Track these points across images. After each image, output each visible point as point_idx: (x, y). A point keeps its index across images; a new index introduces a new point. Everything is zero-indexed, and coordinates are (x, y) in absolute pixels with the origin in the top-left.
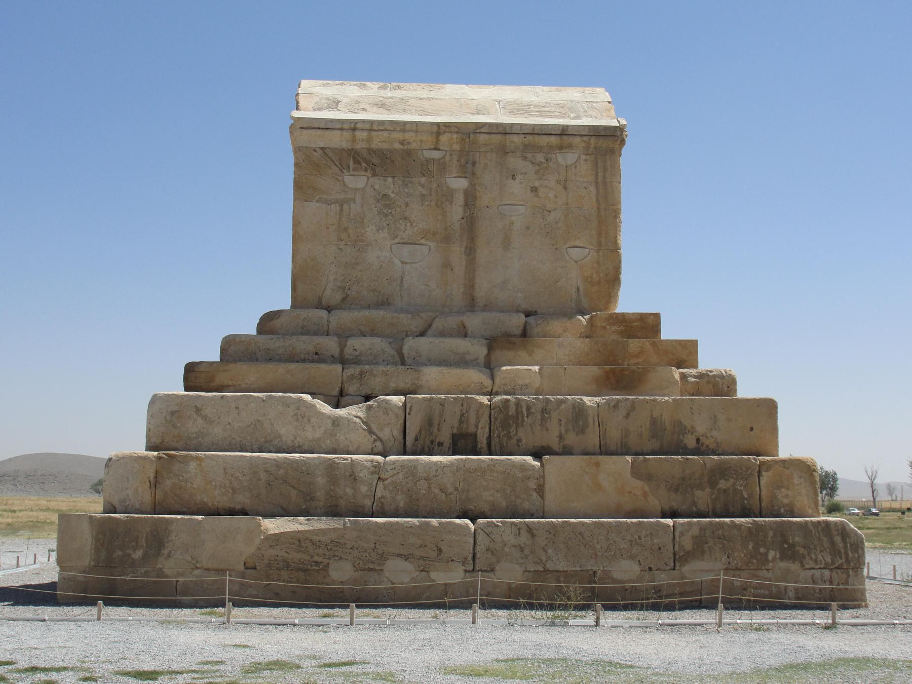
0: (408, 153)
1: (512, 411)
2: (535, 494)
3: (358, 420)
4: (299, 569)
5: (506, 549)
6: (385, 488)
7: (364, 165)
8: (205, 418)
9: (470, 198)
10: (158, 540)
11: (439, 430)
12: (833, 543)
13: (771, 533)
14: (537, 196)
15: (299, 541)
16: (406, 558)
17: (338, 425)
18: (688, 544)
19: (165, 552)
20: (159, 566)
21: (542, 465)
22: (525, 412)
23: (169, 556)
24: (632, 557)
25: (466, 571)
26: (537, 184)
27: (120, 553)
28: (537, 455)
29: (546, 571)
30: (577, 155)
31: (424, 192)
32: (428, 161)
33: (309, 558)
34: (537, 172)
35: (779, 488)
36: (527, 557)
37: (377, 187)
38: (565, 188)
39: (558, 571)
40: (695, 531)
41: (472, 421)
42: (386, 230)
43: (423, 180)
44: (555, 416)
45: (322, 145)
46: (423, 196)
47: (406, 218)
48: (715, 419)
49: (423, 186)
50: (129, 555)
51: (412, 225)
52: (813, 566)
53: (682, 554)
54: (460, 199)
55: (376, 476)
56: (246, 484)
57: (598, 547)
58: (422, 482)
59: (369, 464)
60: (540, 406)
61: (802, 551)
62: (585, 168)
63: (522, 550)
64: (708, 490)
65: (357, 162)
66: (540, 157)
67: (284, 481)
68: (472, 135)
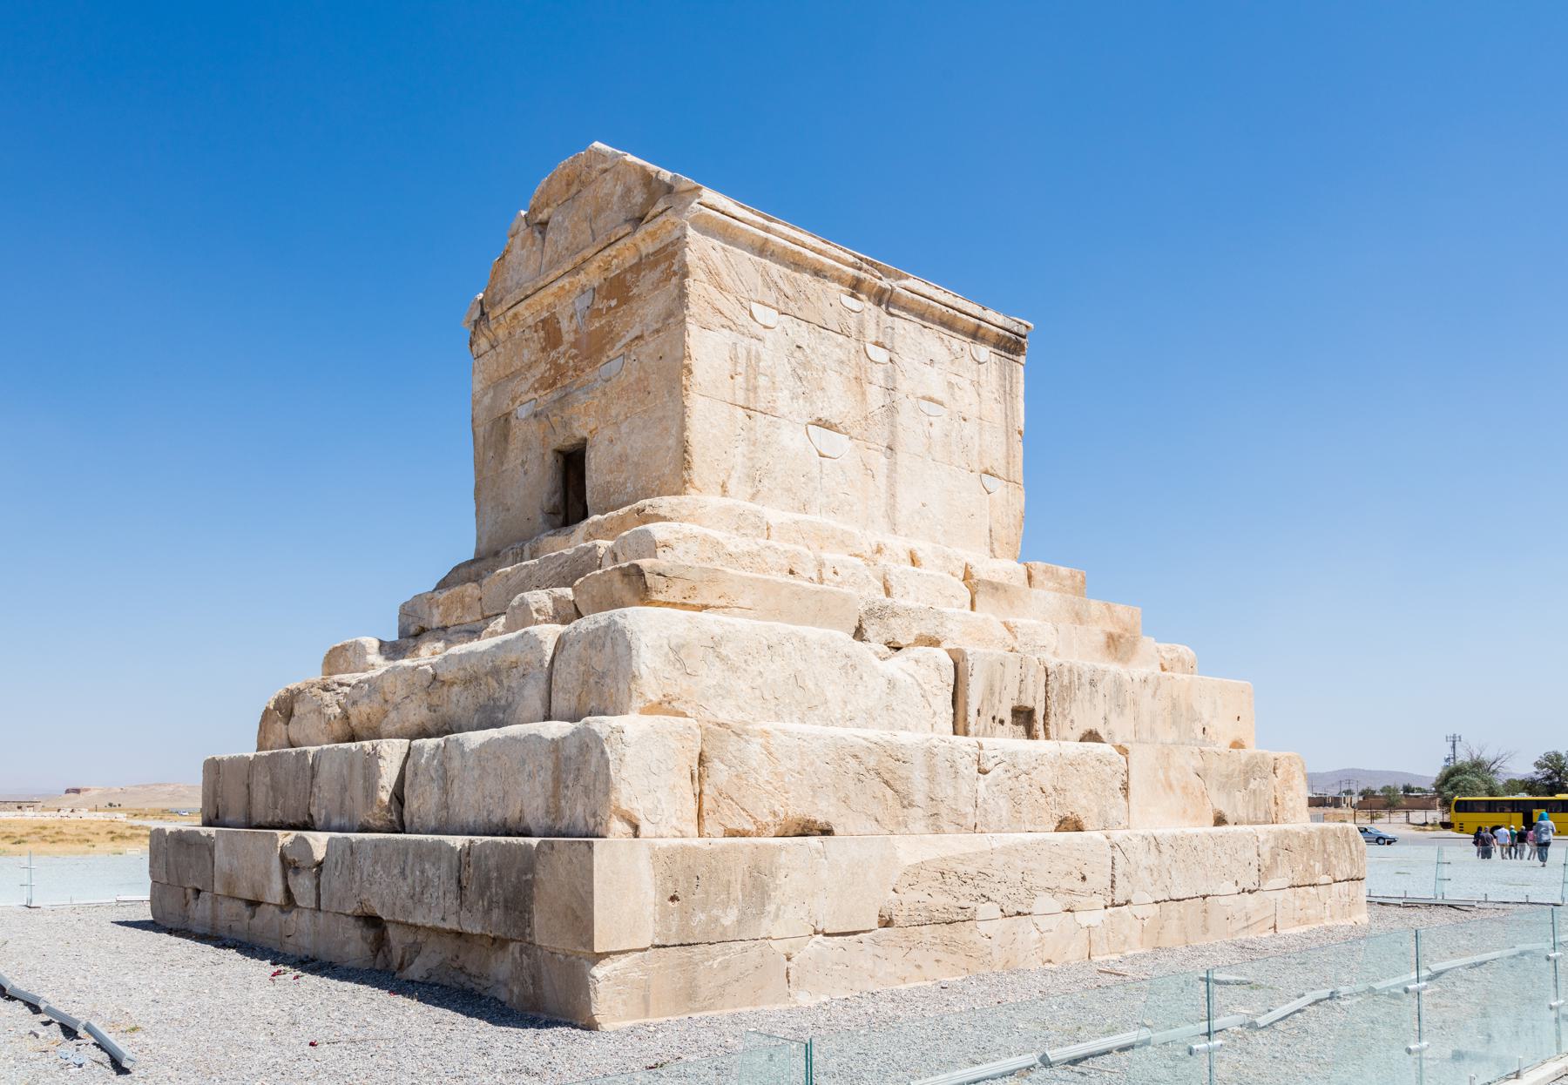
3: (909, 680)
19: (771, 908)
23: (777, 916)
26: (954, 379)
27: (703, 917)
43: (841, 338)
49: (840, 346)
50: (717, 920)
54: (878, 376)
58: (1023, 777)
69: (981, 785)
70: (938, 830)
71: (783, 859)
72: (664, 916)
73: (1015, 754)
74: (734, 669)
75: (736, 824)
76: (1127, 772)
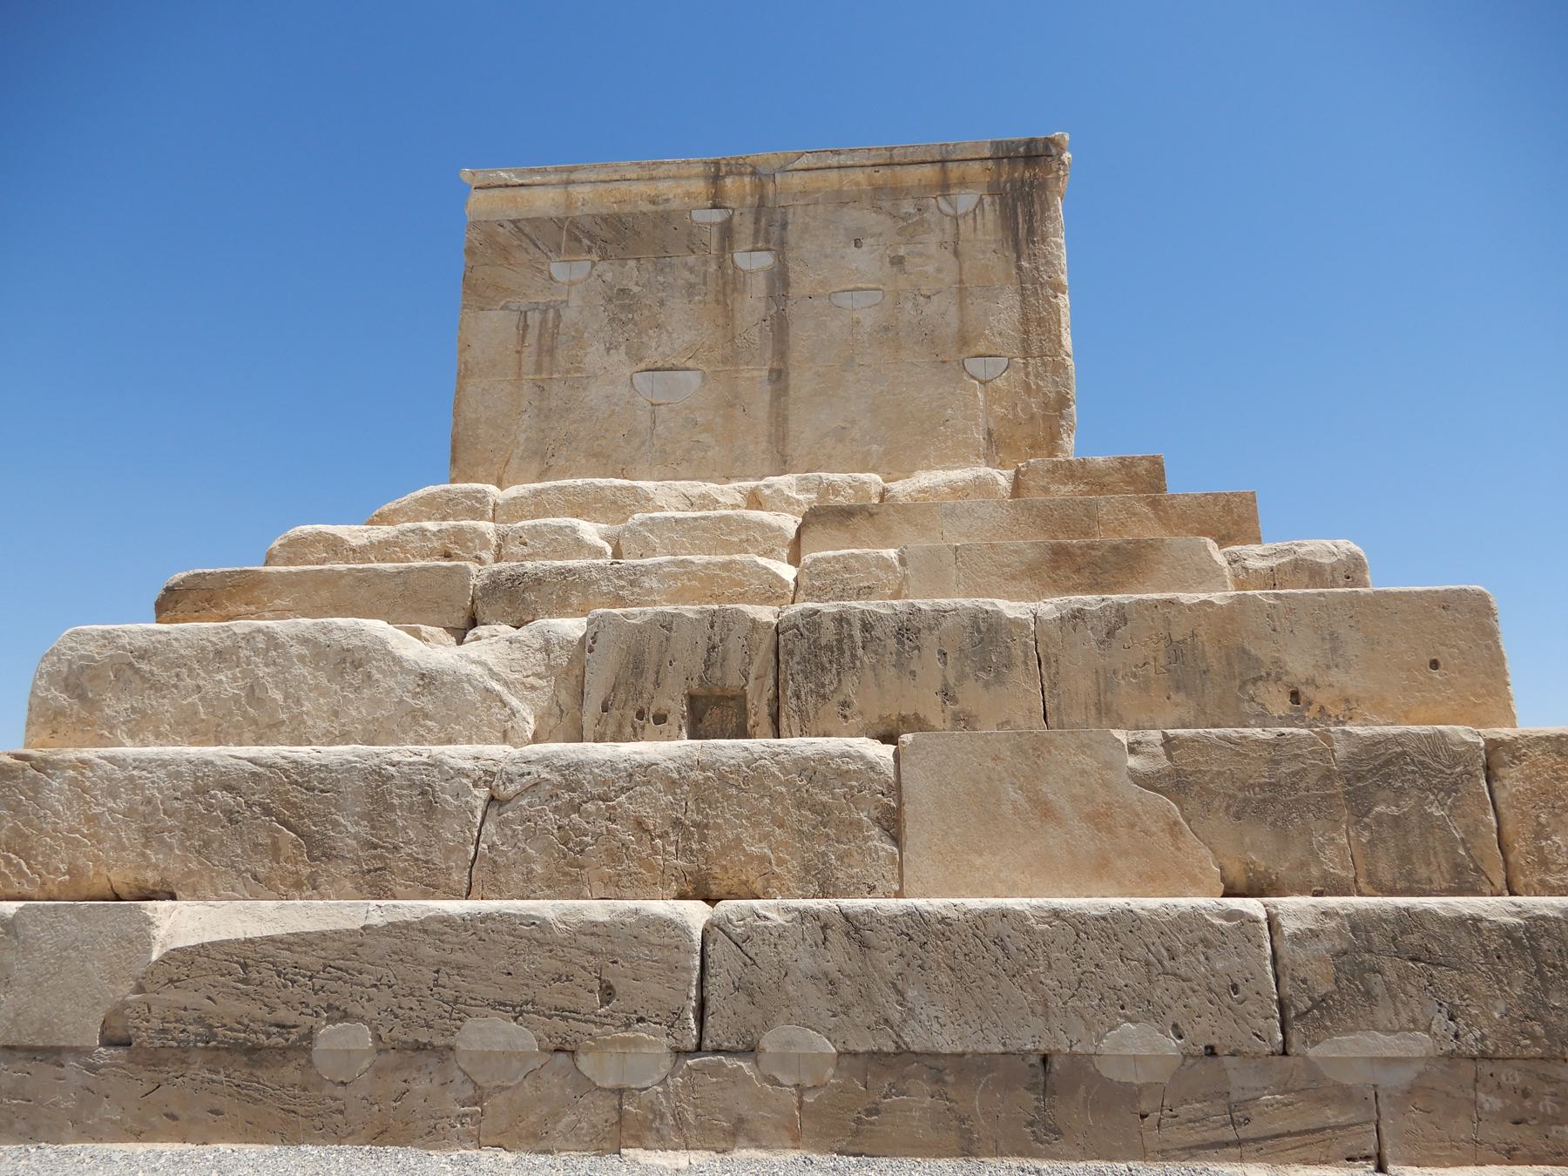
0: (666, 217)
1: (828, 634)
2: (876, 831)
3: (477, 670)
7: (586, 242)
11: (657, 684)
15: (244, 966)
16: (517, 1012)
21: (896, 755)
22: (857, 634)
24: (1153, 1012)
25: (679, 1053)
26: (902, 251)
28: (888, 738)
29: (903, 1054)
30: (976, 198)
31: (692, 278)
36: (846, 1009)
37: (608, 277)
38: (956, 253)
39: (937, 1055)
41: (735, 662)
43: (691, 259)
44: (929, 641)
45: (514, 216)
46: (692, 286)
48: (1334, 637)
49: (691, 270)
51: (670, 334)
53: (1303, 1004)
54: (759, 286)
55: (483, 793)
59: (468, 765)
67: (267, 811)
68: (778, 177)
73: (578, 766)
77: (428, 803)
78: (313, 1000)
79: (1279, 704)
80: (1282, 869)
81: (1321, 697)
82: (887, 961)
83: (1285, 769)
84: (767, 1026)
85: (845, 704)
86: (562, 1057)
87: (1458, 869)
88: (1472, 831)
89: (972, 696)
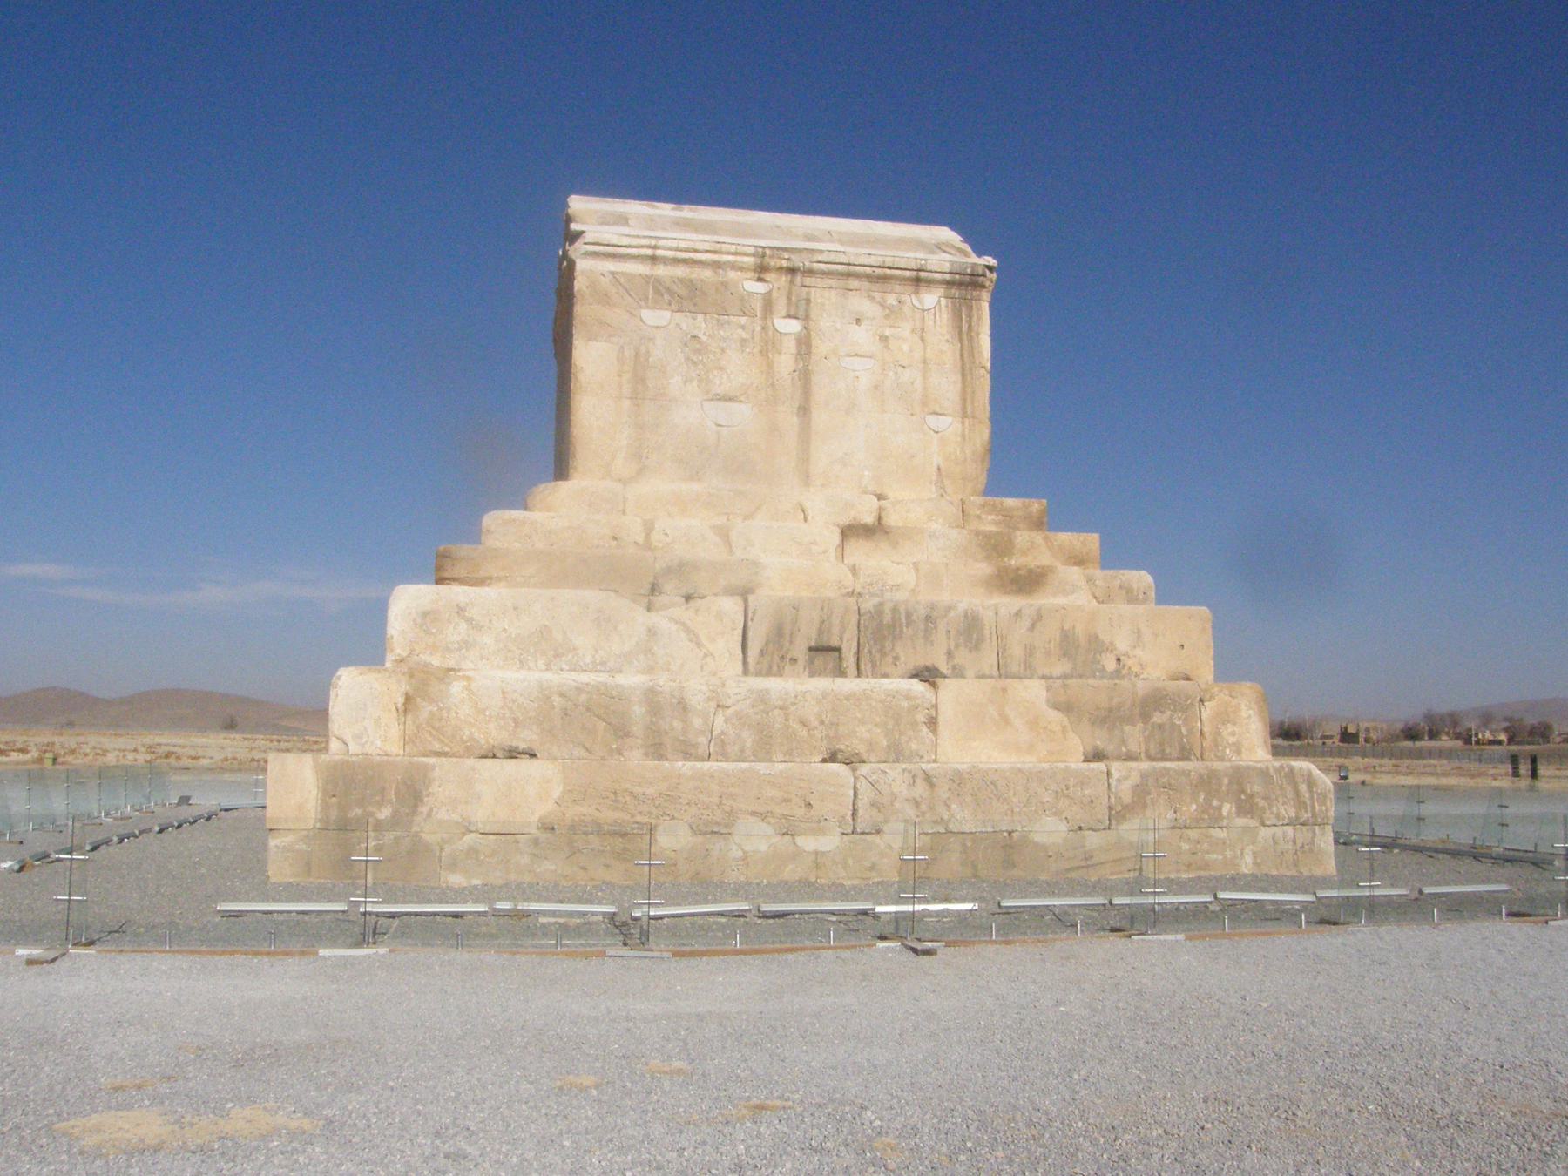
1: (887, 617)
2: (925, 729)
4: (613, 834)
5: (897, 805)
6: (726, 721)
7: (666, 297)
8: (470, 621)
9: (804, 345)
10: (413, 792)
11: (791, 642)
12: (1297, 792)
13: (1226, 781)
14: (887, 347)
16: (763, 816)
17: (655, 634)
18: (1126, 795)
19: (424, 809)
20: (415, 829)
24: (1057, 813)
26: (887, 333)
31: (745, 335)
32: (750, 294)
33: (628, 817)
34: (887, 317)
35: (1225, 722)
36: (923, 814)
40: (1135, 779)
41: (835, 630)
42: (695, 383)
43: (743, 320)
44: (942, 626)
46: (743, 341)
47: (721, 369)
48: (1139, 631)
49: (743, 327)
50: (372, 814)
52: (1274, 821)
54: (790, 346)
55: (713, 704)
56: (532, 714)
57: (1015, 800)
60: (922, 612)
61: (1262, 803)
62: (945, 316)
63: (917, 804)
64: (1140, 725)
65: (657, 292)
66: (891, 300)
67: (588, 709)
69: (719, 721)
70: (660, 757)
71: (437, 773)
72: (325, 806)
73: (767, 691)
74: (478, 628)
75: (437, 746)
76: (935, 706)
77: (683, 707)
78: (655, 811)
79: (1111, 665)
80: (1110, 748)
81: (1129, 662)
82: (943, 793)
83: (1115, 701)
84: (886, 821)
85: (896, 658)
86: (787, 838)
87: (1183, 748)
88: (1190, 731)
89: (963, 657)
